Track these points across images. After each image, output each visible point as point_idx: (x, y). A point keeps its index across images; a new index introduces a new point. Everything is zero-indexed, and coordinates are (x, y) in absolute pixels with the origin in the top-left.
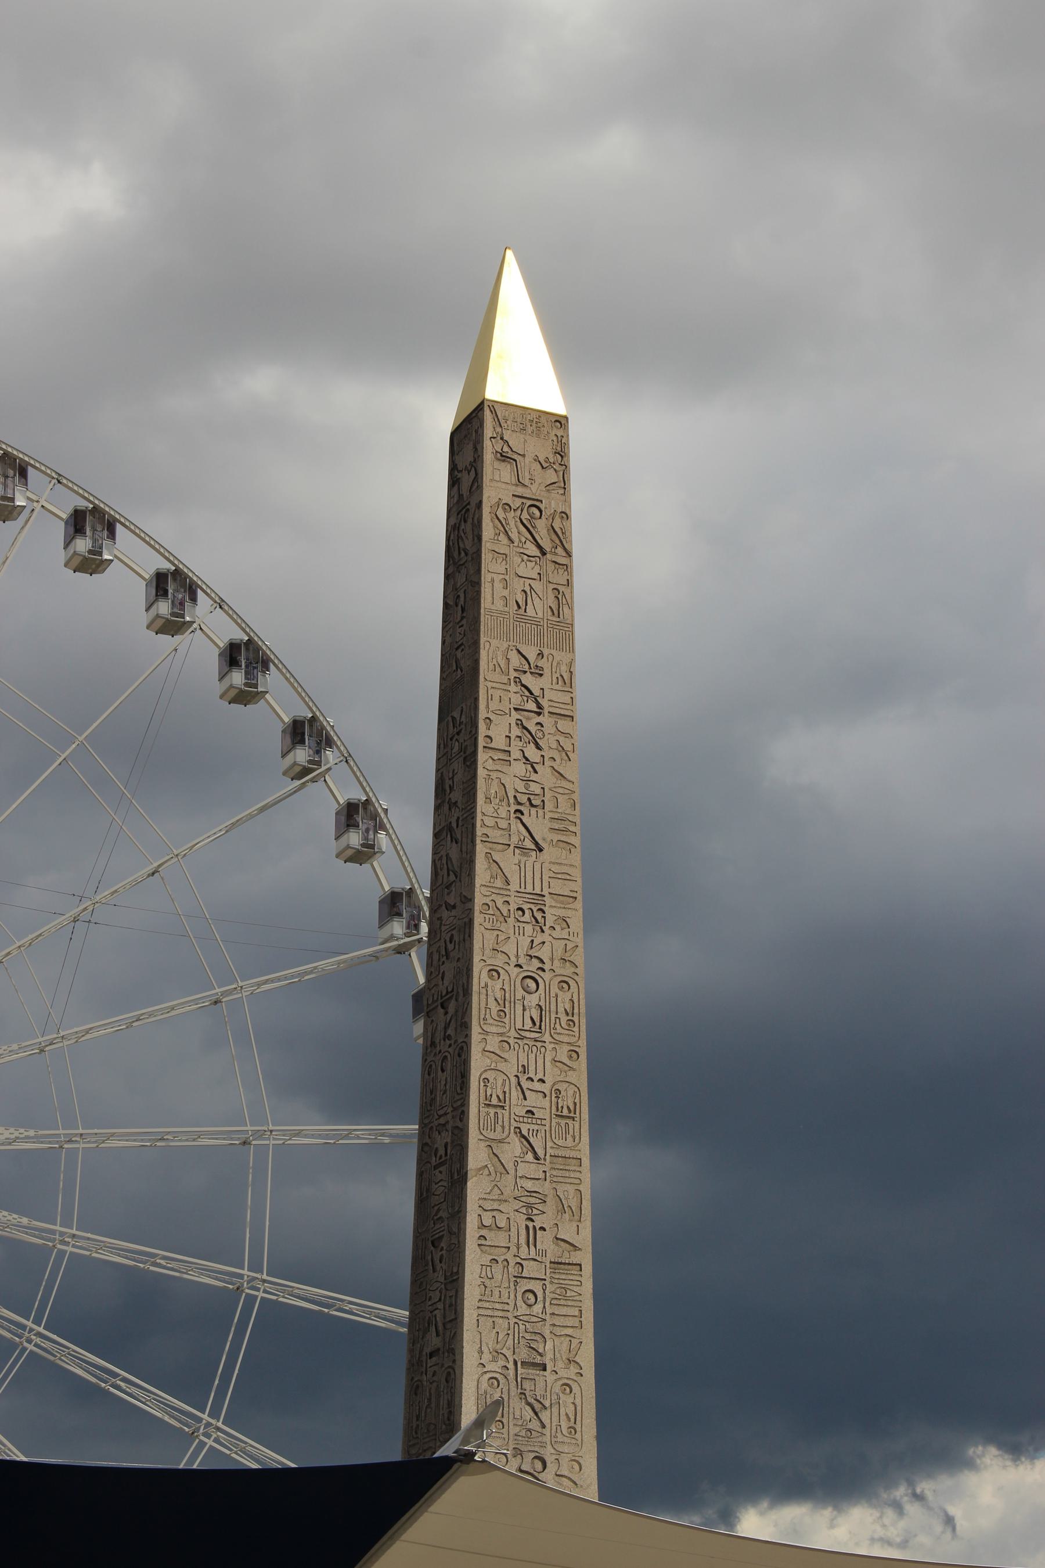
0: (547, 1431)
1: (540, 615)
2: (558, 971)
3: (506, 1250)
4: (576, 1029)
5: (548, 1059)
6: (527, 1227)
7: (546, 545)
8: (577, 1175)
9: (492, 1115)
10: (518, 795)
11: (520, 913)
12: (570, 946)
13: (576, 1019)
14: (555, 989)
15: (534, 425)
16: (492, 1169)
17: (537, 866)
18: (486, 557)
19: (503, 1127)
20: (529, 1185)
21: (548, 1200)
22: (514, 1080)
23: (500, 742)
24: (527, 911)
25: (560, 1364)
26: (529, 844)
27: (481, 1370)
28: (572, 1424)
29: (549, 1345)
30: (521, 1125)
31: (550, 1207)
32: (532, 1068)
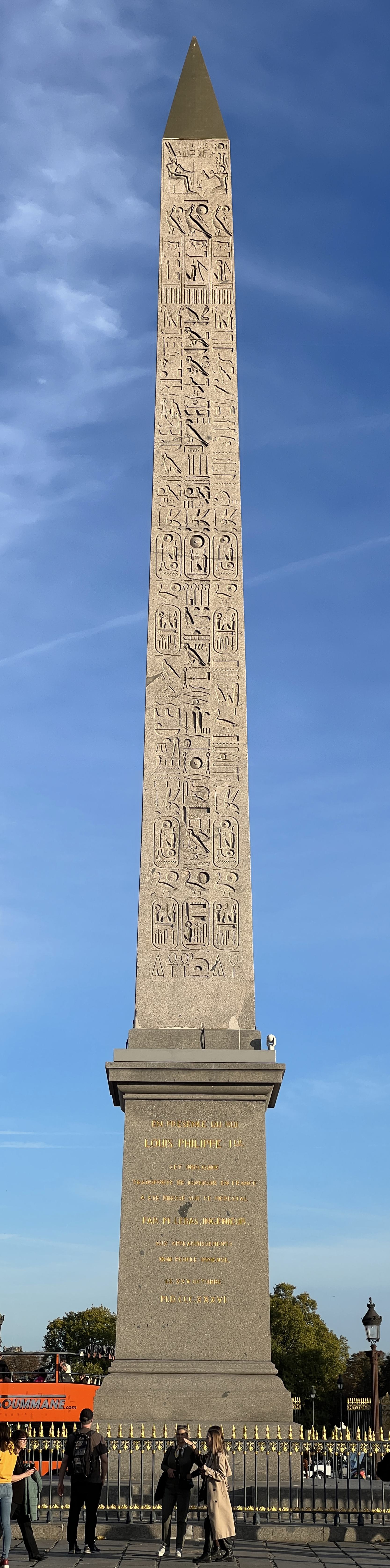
0: (210, 855)
1: (206, 280)
6: (194, 713)
7: (212, 230)
10: (187, 409)
13: (235, 562)
17: (204, 458)
20: (195, 684)
22: (183, 610)
24: (195, 490)
26: (197, 442)
28: (231, 848)
30: (189, 642)
31: (214, 696)
32: (198, 600)
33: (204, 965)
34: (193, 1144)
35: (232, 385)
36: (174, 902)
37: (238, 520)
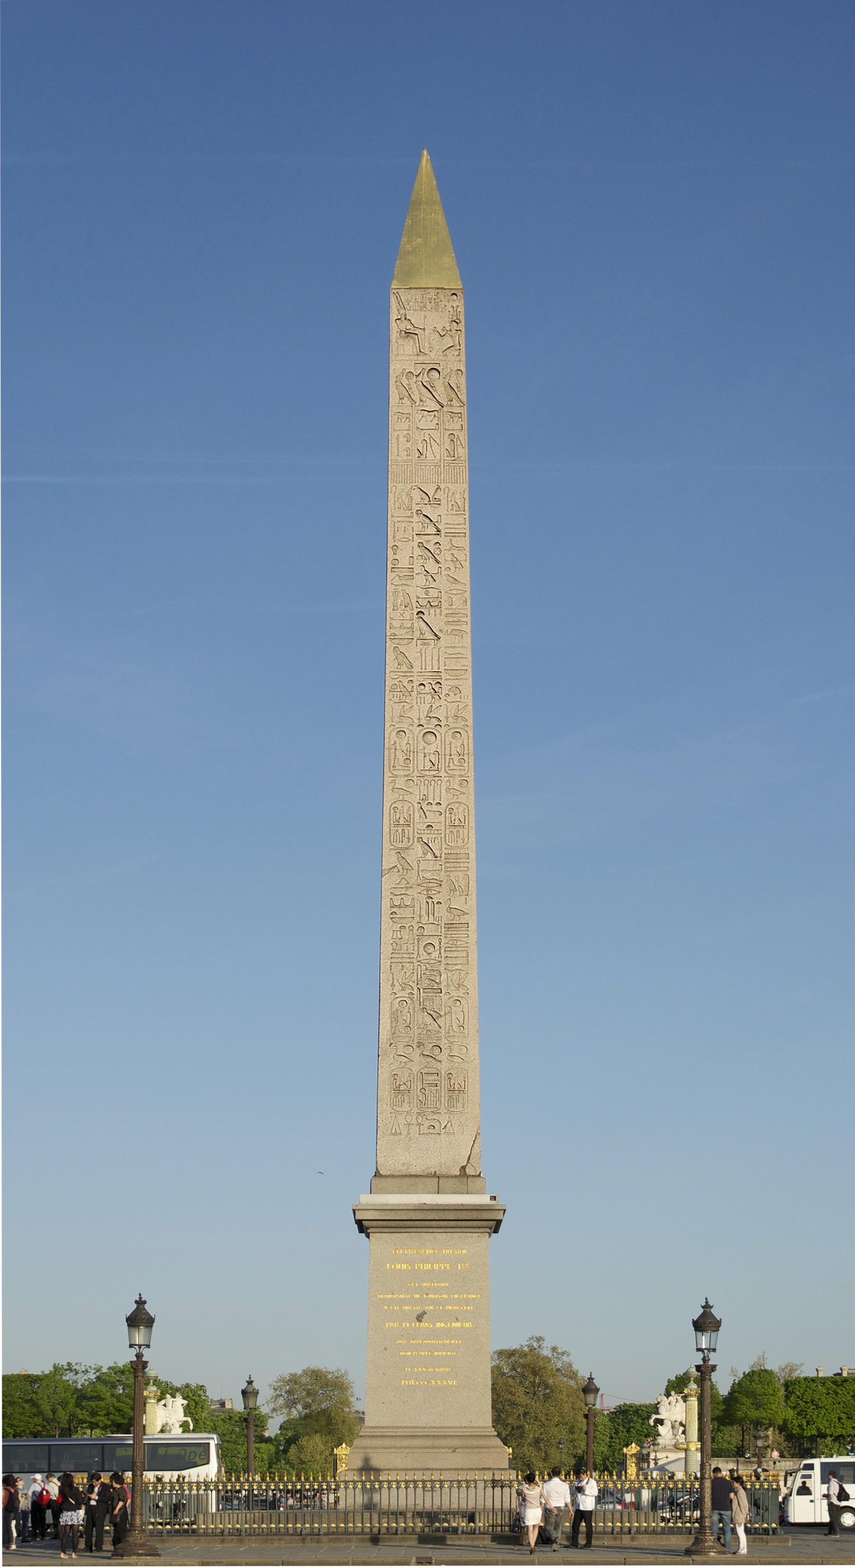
2: (452, 725)
3: (411, 920)
4: (466, 765)
5: (444, 788)
8: (466, 865)
9: (400, 831)
11: (422, 687)
12: (461, 706)
13: (466, 757)
14: (449, 738)
15: (433, 301)
16: (400, 868)
17: (436, 651)
18: (393, 419)
19: (409, 839)
20: (428, 875)
21: (443, 883)
23: (404, 562)
25: (452, 988)
26: (429, 635)
27: (393, 996)
29: (444, 977)
31: (445, 889)
32: (431, 796)
33: (436, 1125)
34: (428, 1266)
35: (464, 575)
36: (409, 1071)
37: (469, 715)
